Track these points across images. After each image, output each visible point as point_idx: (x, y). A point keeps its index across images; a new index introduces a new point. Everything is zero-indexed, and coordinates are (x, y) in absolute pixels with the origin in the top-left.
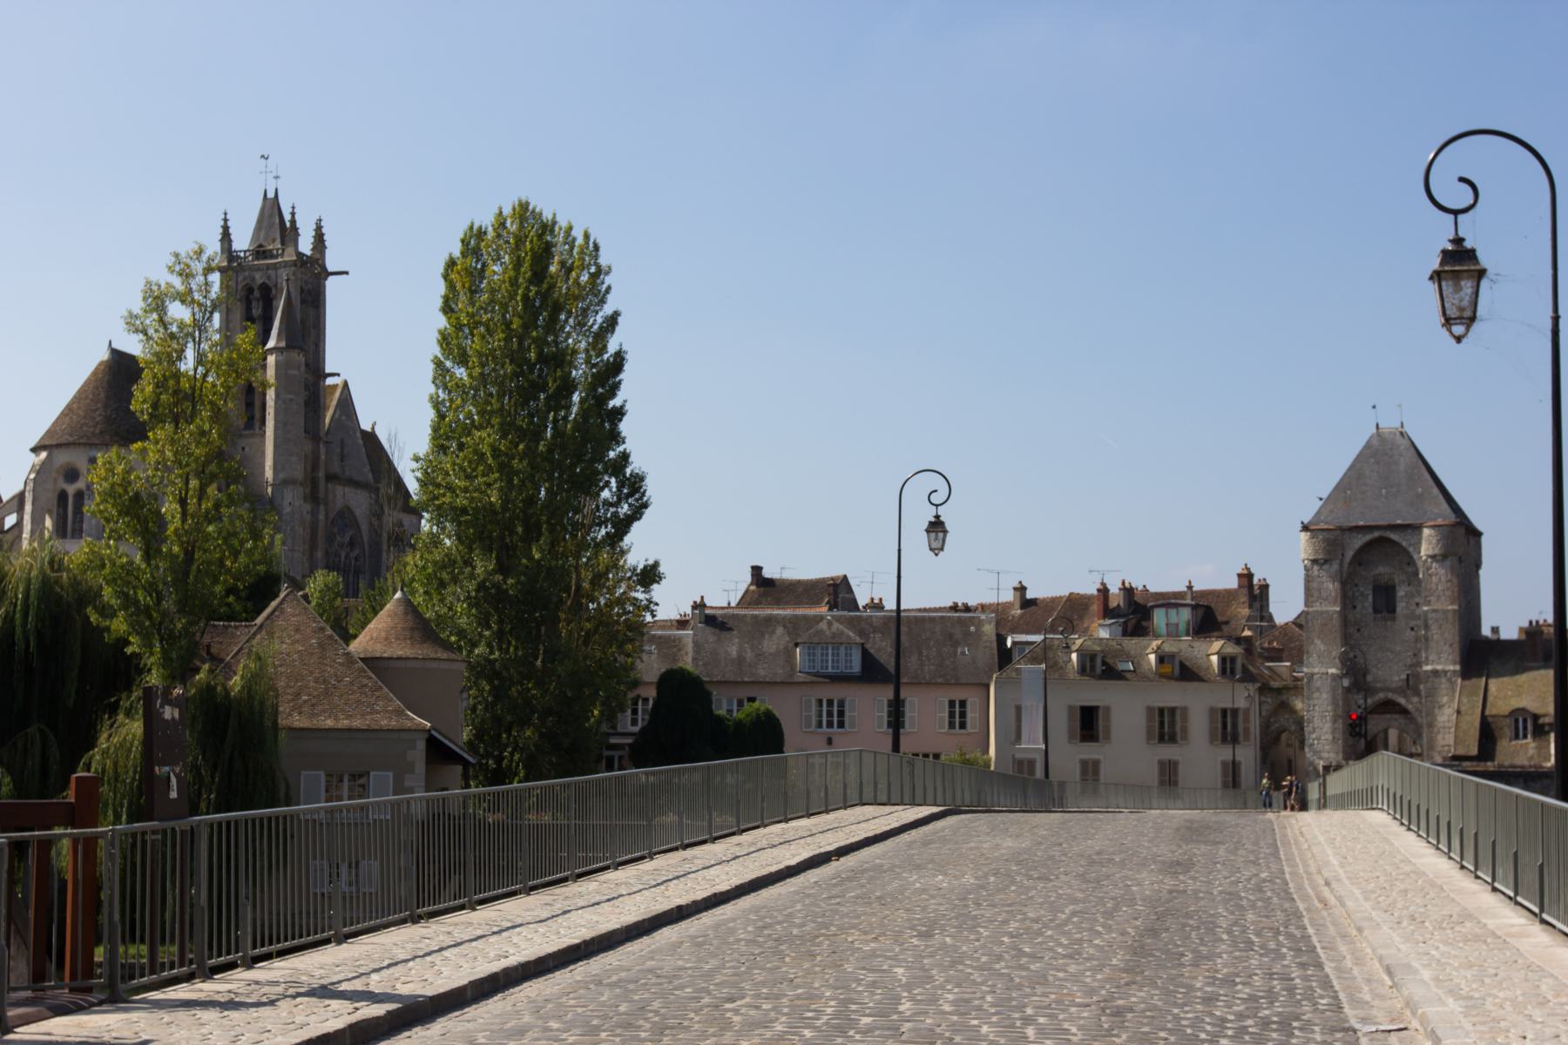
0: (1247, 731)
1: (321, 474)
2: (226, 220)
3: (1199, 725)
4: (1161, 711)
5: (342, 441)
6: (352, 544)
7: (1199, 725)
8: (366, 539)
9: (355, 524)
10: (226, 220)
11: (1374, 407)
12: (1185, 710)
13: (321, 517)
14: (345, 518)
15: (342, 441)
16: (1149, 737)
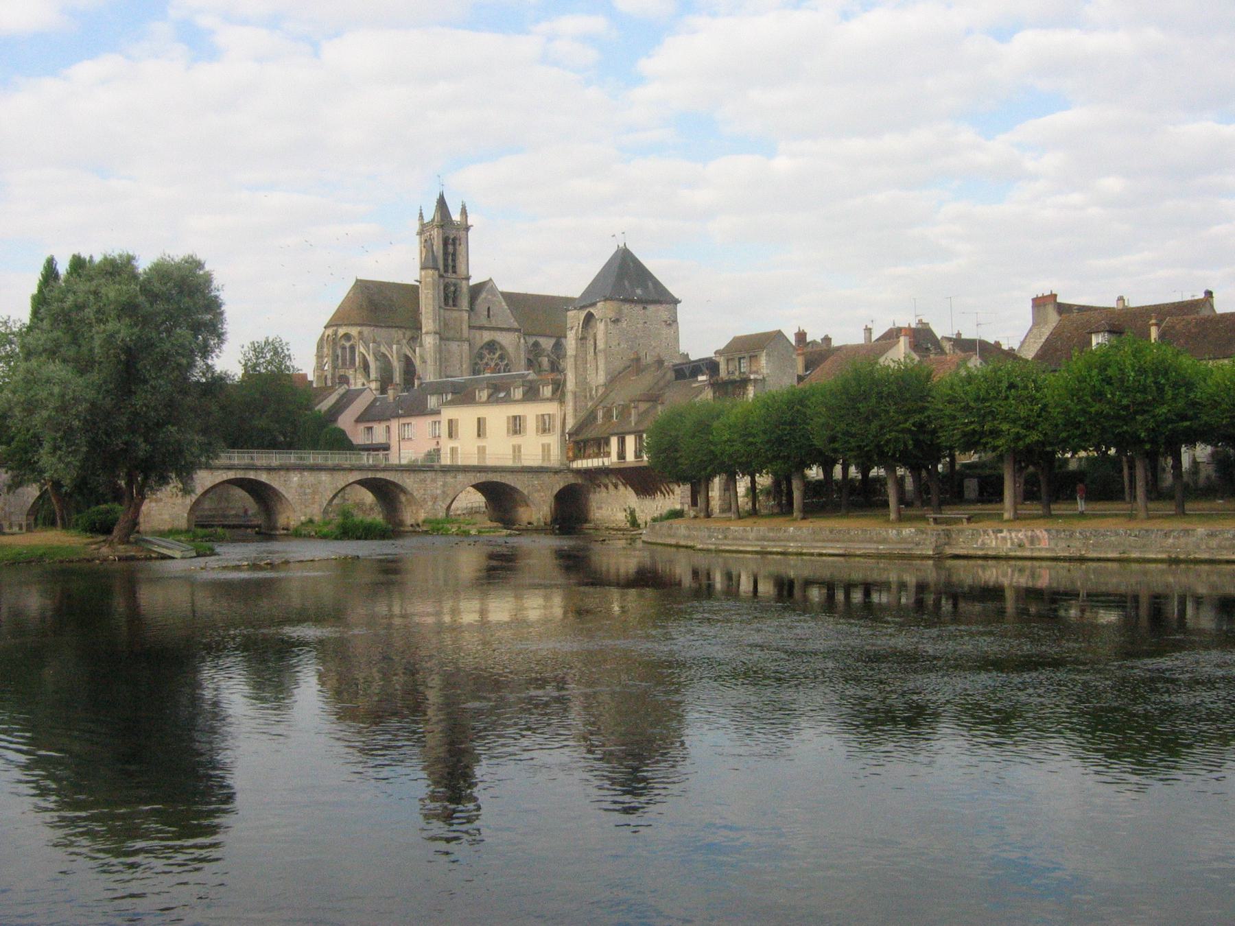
0: (554, 427)
1: (465, 327)
2: (421, 210)
3: (531, 424)
4: (543, 415)
5: (489, 308)
6: (501, 358)
7: (531, 424)
8: (512, 355)
9: (502, 348)
10: (421, 210)
11: (614, 236)
12: (525, 417)
13: (466, 346)
14: (492, 346)
15: (489, 308)
16: (537, 431)
